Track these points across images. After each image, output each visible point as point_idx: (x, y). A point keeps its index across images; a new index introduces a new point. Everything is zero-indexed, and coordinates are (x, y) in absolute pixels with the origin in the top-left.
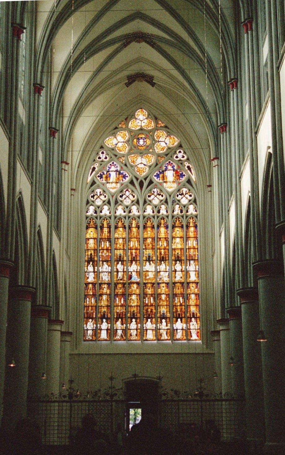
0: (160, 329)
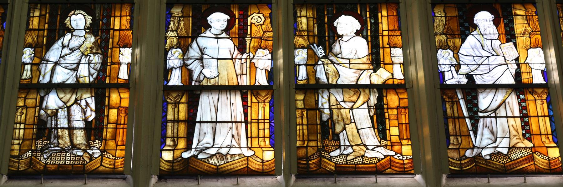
0: (314, 87)
